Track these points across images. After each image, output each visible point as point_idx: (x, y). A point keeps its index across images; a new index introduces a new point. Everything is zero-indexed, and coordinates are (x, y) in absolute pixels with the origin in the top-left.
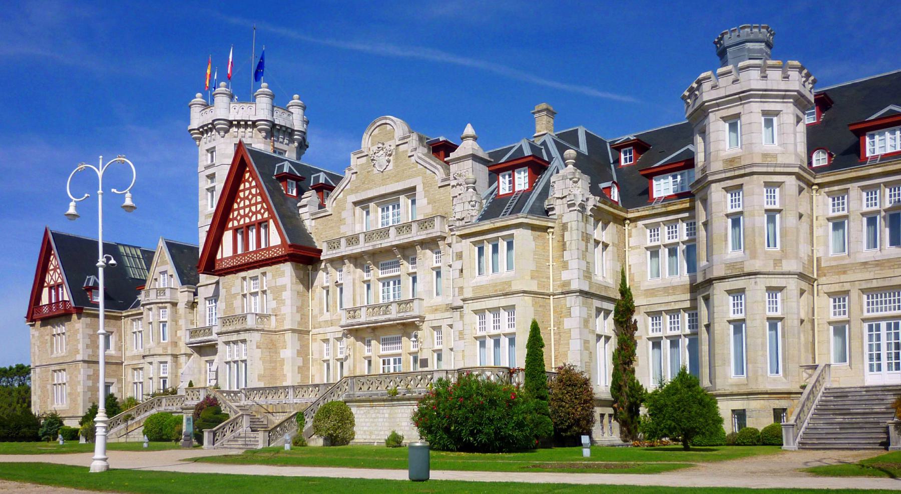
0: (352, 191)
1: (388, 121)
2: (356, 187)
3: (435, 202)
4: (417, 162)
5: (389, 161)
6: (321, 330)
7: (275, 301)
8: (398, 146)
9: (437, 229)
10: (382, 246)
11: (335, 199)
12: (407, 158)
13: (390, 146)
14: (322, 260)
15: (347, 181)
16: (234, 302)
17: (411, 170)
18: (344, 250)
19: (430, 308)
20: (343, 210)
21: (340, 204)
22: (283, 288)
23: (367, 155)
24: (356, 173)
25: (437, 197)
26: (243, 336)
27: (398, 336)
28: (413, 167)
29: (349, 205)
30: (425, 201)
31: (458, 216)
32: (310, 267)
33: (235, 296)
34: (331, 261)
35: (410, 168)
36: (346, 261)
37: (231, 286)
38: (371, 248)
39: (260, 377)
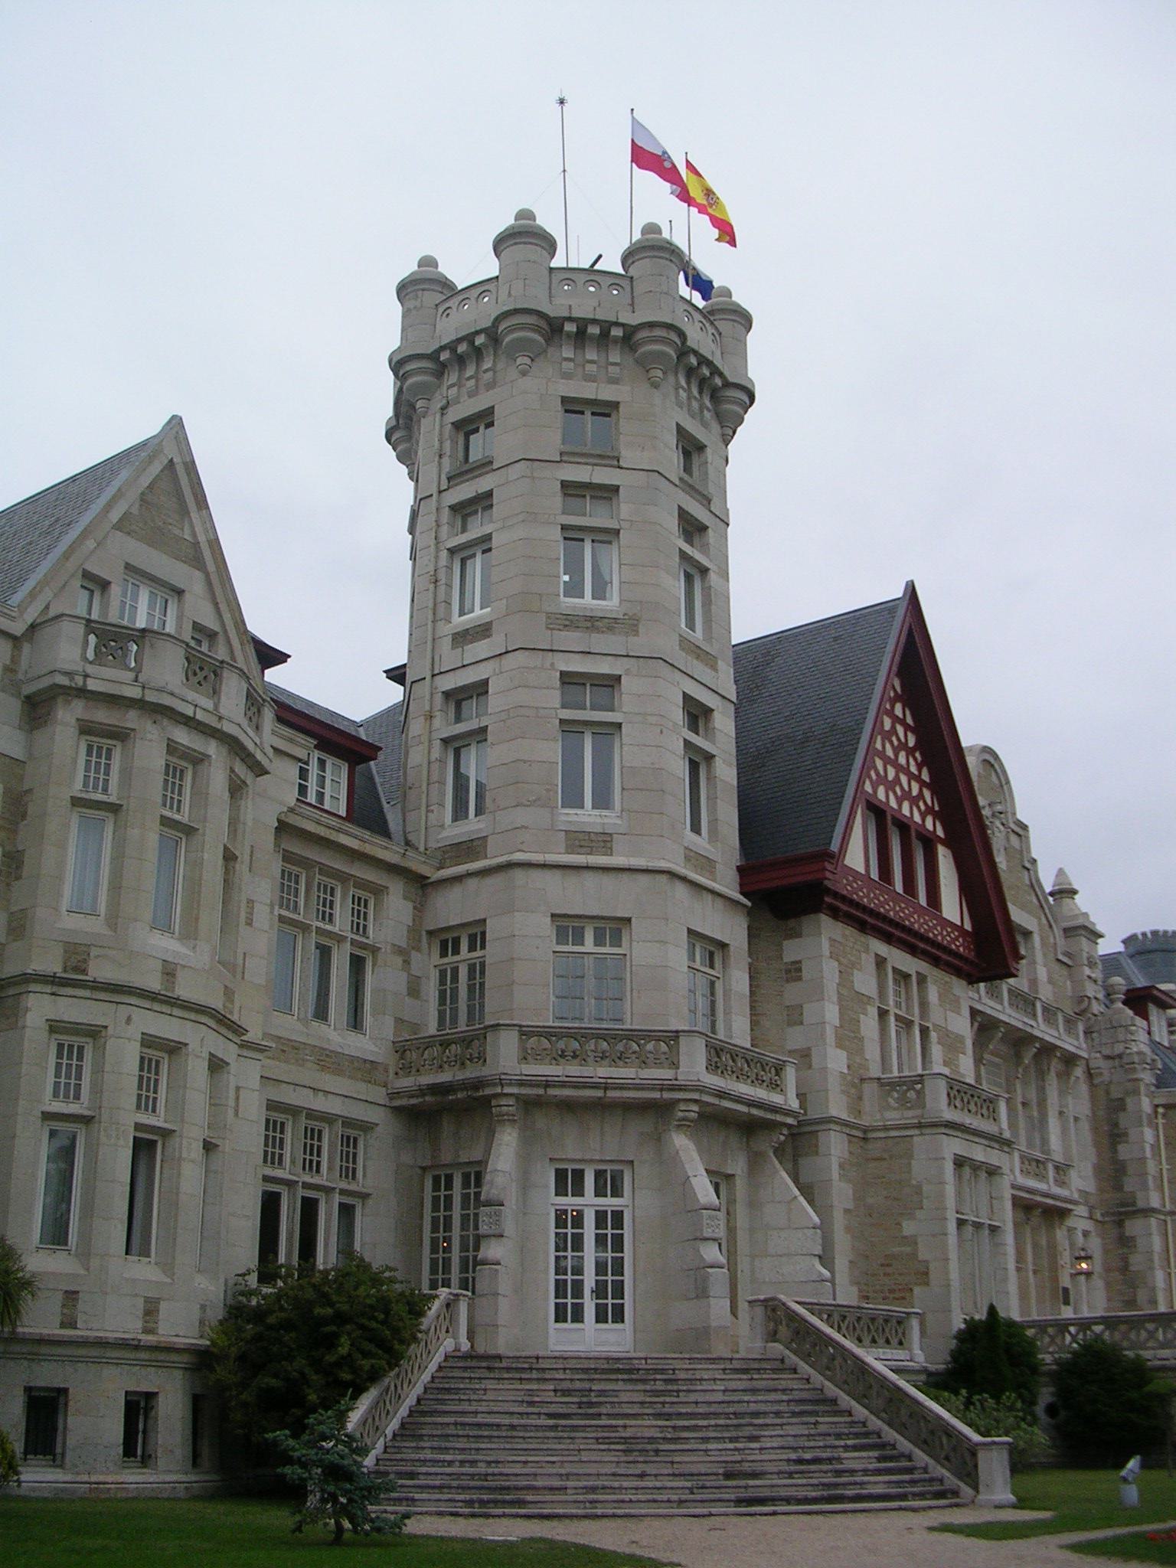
1: (996, 766)
4: (1032, 886)
12: (1020, 868)
33: (862, 999)
37: (853, 965)
38: (1020, 1025)
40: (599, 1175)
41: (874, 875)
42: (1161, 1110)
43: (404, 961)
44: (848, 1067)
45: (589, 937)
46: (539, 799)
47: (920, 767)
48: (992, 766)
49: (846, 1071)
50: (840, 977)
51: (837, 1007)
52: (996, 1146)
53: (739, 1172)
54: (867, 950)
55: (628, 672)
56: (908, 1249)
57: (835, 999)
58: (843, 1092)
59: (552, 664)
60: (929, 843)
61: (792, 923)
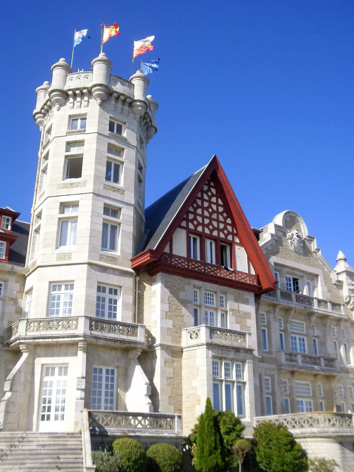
7: (238, 325)
23: (283, 232)
36: (277, 309)
37: (180, 290)
40: (60, 368)
41: (199, 259)
43: (15, 303)
45: (63, 287)
46: (49, 245)
47: (225, 219)
49: (172, 327)
53: (122, 365)
54: (189, 284)
55: (81, 199)
56: (194, 392)
57: (167, 302)
59: (58, 200)
60: (231, 244)
61: (154, 277)
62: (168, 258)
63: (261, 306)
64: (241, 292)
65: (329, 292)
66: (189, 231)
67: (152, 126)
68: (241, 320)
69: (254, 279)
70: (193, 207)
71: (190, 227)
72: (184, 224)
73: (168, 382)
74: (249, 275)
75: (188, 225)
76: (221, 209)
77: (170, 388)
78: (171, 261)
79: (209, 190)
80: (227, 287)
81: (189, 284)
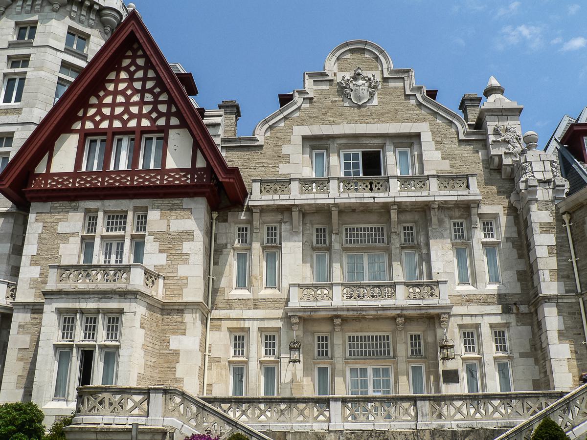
0: (302, 122)
2: (311, 117)
3: (454, 158)
4: (420, 105)
5: (372, 95)
6: (233, 314)
8: (385, 80)
9: (475, 190)
10: (377, 200)
11: (271, 127)
13: (373, 76)
14: (250, 210)
15: (295, 107)
16: (62, 245)
17: (412, 112)
18: (295, 195)
19: (459, 298)
20: (285, 143)
21: (279, 135)
22: (188, 236)
23: (332, 81)
24: (311, 99)
25: (456, 152)
26: (113, 305)
27: (386, 334)
28: (413, 110)
29: (297, 139)
30: (438, 155)
31: (539, 176)
32: (215, 215)
34: (264, 210)
35: (407, 110)
36: (295, 215)
39: (141, 377)
42: (565, 217)
44: (41, 274)
48: (364, 49)
49: (38, 276)
50: (43, 229)
51: (36, 246)
52: (117, 296)
54: (76, 209)
58: (32, 288)
62: (42, 180)
63: (256, 216)
64: (176, 201)
65: (443, 158)
66: (85, 135)
67: (102, 8)
68: (171, 246)
69: (203, 175)
70: (98, 97)
71: (86, 127)
72: (78, 126)
73: (20, 355)
74: (193, 170)
75: (83, 125)
76: (150, 85)
77: (22, 363)
78: (46, 183)
79: (133, 63)
80: (148, 200)
81: (78, 209)
